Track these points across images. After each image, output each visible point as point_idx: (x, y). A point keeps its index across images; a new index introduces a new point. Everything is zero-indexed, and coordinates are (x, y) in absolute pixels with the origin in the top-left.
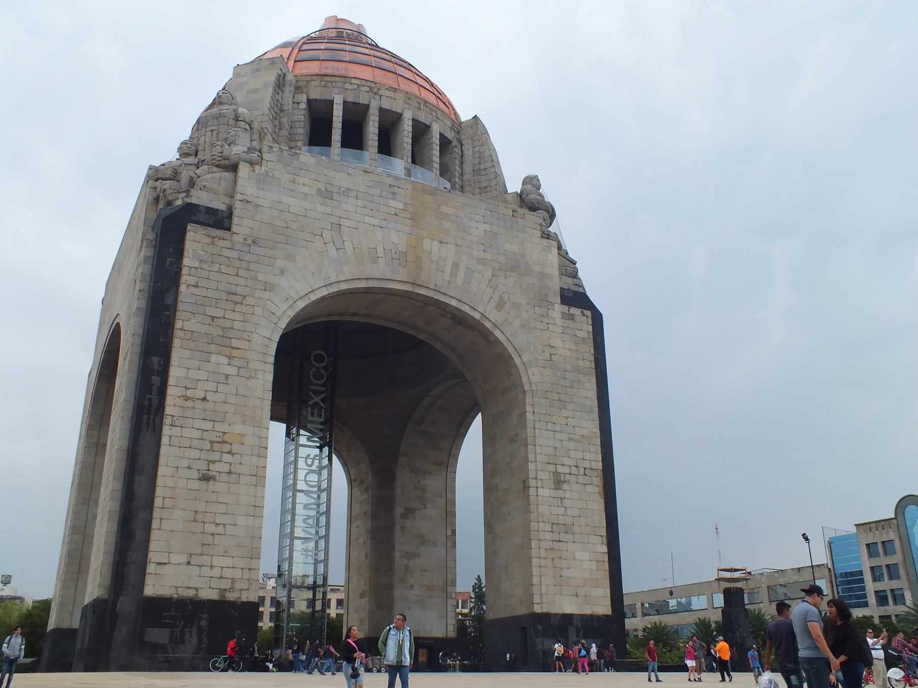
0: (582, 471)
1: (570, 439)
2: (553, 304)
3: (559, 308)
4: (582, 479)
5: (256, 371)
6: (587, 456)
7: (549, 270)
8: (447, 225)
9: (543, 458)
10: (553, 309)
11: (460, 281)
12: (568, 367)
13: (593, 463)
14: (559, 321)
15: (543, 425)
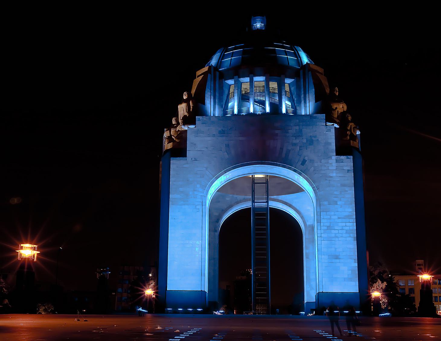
0: (344, 231)
1: (339, 218)
2: (330, 157)
3: (334, 157)
4: (344, 235)
5: (199, 209)
6: (348, 224)
7: (330, 141)
8: (277, 132)
9: (325, 228)
10: (332, 159)
11: (284, 155)
12: (339, 185)
13: (351, 227)
14: (334, 164)
15: (325, 213)
